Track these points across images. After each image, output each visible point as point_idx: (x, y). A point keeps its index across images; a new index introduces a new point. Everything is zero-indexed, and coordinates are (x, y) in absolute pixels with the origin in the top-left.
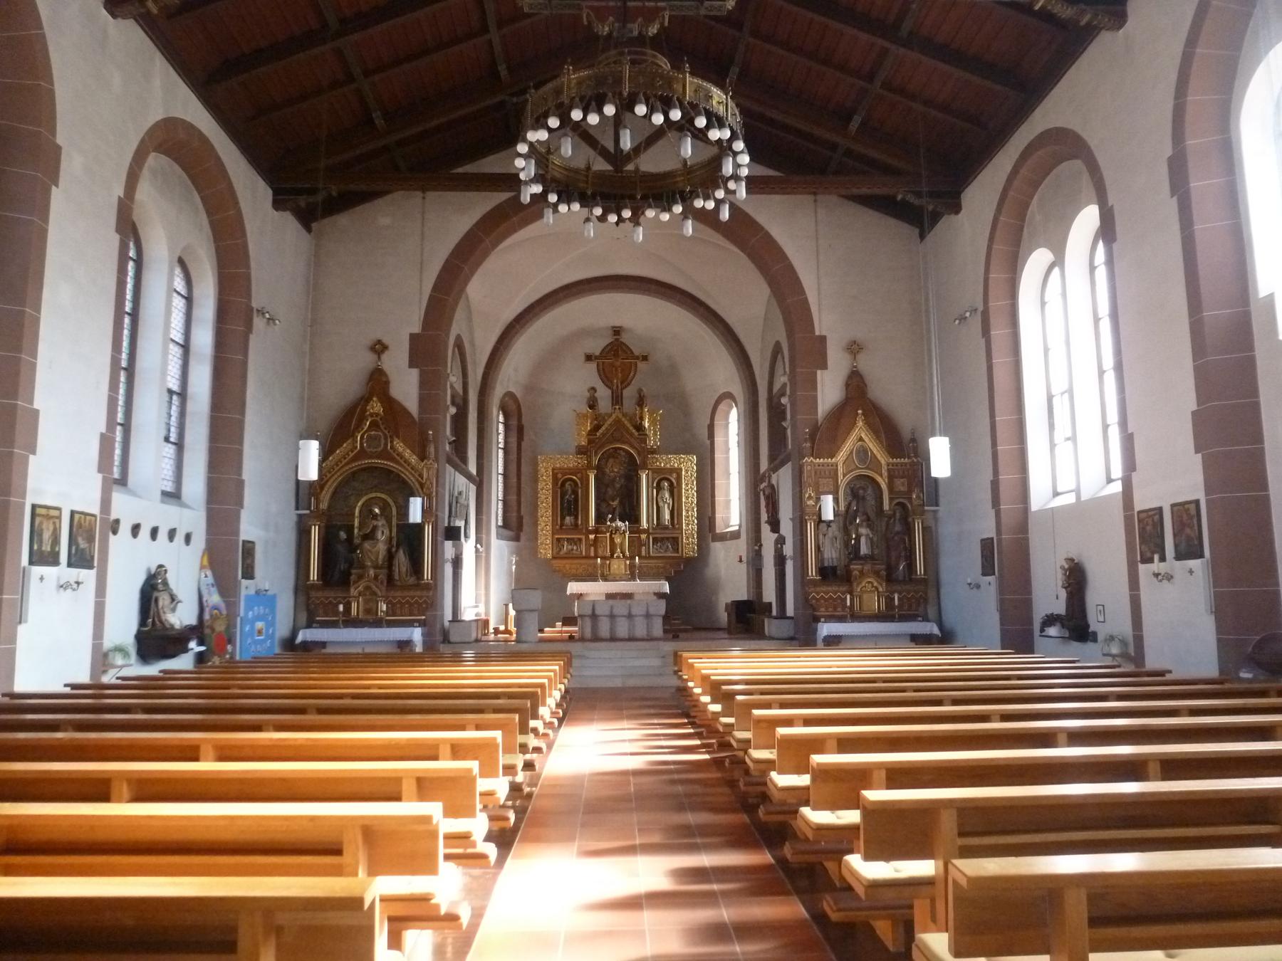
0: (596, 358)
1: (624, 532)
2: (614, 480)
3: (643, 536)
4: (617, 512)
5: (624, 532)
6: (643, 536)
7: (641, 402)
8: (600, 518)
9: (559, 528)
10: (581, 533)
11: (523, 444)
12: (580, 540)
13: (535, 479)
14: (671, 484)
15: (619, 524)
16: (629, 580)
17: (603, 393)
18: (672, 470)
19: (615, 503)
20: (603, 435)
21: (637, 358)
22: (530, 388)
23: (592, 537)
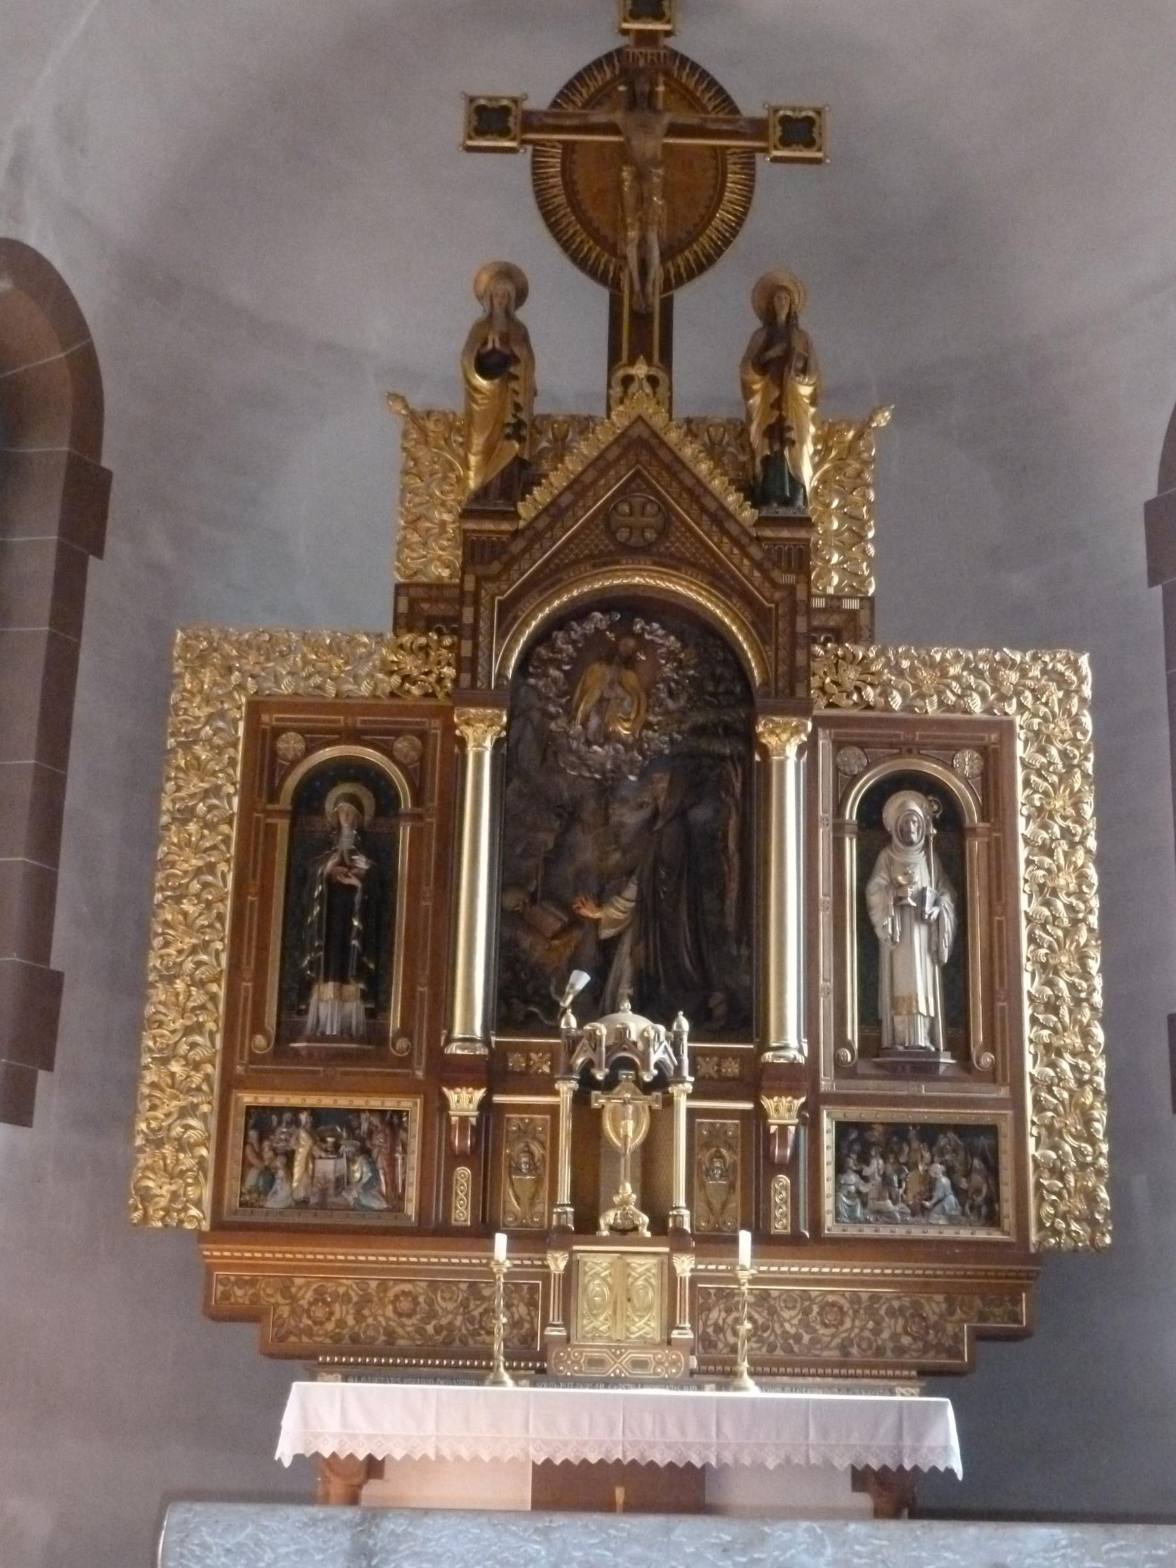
0: (530, 122)
1: (662, 1082)
2: (607, 788)
3: (782, 1110)
4: (623, 966)
5: (662, 1082)
6: (782, 1110)
7: (776, 351)
8: (522, 996)
9: (267, 1030)
10: (411, 1089)
11: (100, 577)
12: (394, 1122)
13: (144, 773)
14: (949, 824)
15: (637, 1025)
16: (694, 1379)
17: (568, 331)
18: (949, 735)
19: (615, 913)
20: (555, 512)
21: (758, 128)
22: (151, 280)
23: (464, 1101)
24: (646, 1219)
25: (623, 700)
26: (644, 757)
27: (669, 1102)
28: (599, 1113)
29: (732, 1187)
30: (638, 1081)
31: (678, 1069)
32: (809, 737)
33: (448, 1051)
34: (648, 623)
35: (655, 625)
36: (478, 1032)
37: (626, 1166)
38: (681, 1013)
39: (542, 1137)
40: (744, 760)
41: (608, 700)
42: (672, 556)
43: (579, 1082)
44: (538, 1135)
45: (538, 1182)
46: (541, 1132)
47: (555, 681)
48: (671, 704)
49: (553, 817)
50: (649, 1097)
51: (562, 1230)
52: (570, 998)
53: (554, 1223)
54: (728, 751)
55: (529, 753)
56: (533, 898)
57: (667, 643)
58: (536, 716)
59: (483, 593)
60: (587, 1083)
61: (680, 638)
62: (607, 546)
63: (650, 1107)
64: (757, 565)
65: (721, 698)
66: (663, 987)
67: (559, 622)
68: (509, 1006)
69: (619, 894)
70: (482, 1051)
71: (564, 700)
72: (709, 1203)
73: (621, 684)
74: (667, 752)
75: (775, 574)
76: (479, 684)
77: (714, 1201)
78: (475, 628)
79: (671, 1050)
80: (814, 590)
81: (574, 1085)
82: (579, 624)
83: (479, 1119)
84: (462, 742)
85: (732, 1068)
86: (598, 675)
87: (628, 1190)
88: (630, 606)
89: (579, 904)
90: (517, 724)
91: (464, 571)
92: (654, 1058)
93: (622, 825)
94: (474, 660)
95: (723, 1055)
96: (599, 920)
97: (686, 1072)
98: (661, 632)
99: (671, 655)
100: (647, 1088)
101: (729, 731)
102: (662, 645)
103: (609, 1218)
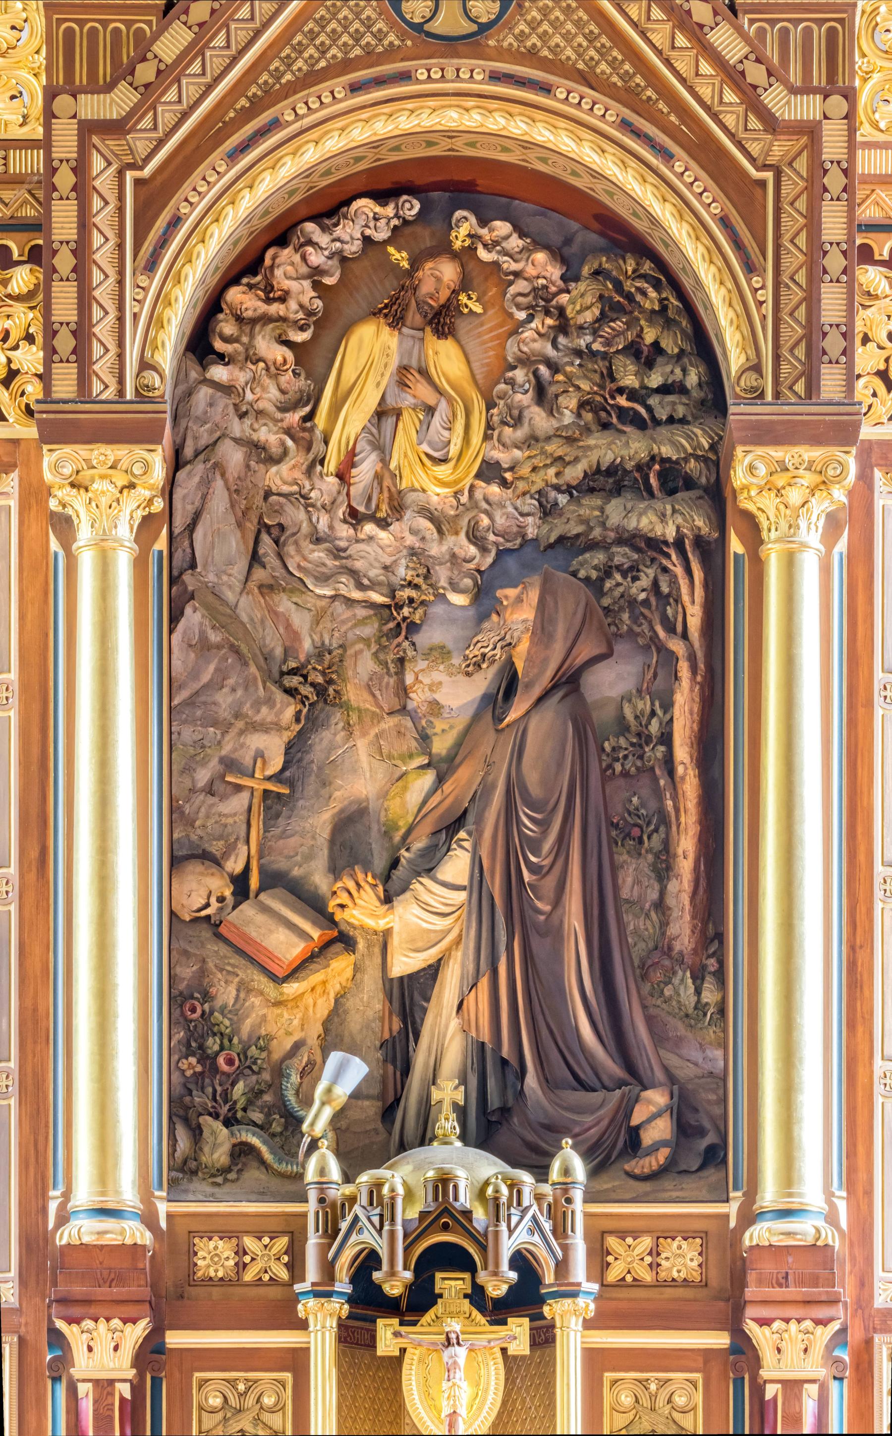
5: (527, 1294)
25: (430, 410)
26: (484, 550)
27: (544, 1337)
30: (477, 1296)
31: (562, 1267)
32: (850, 494)
33: (64, 1237)
34: (483, 222)
35: (502, 227)
36: (128, 1193)
38: (567, 1142)
40: (711, 552)
41: (398, 414)
42: (531, 56)
43: (351, 1300)
47: (275, 371)
48: (539, 419)
49: (279, 696)
52: (327, 1113)
54: (670, 533)
55: (221, 547)
56: (240, 883)
57: (531, 271)
58: (234, 457)
59: (97, 163)
61: (558, 254)
62: (379, 36)
64: (733, 76)
65: (653, 401)
66: (531, 1080)
67: (280, 231)
68: (196, 1133)
69: (430, 871)
70: (135, 1232)
71: (294, 418)
73: (424, 373)
74: (531, 532)
75: (775, 99)
76: (97, 387)
78: (82, 250)
79: (547, 1226)
80: (865, 132)
82: (324, 229)
83: (137, 1388)
84: (63, 525)
85: (683, 1260)
86: (371, 350)
88: (441, 186)
89: (343, 898)
90: (190, 480)
91: (49, 115)
93: (435, 707)
94: (82, 332)
95: (663, 1232)
96: (387, 934)
98: (515, 243)
99: (542, 300)
100: (497, 1311)
101: (672, 480)
102: (517, 274)
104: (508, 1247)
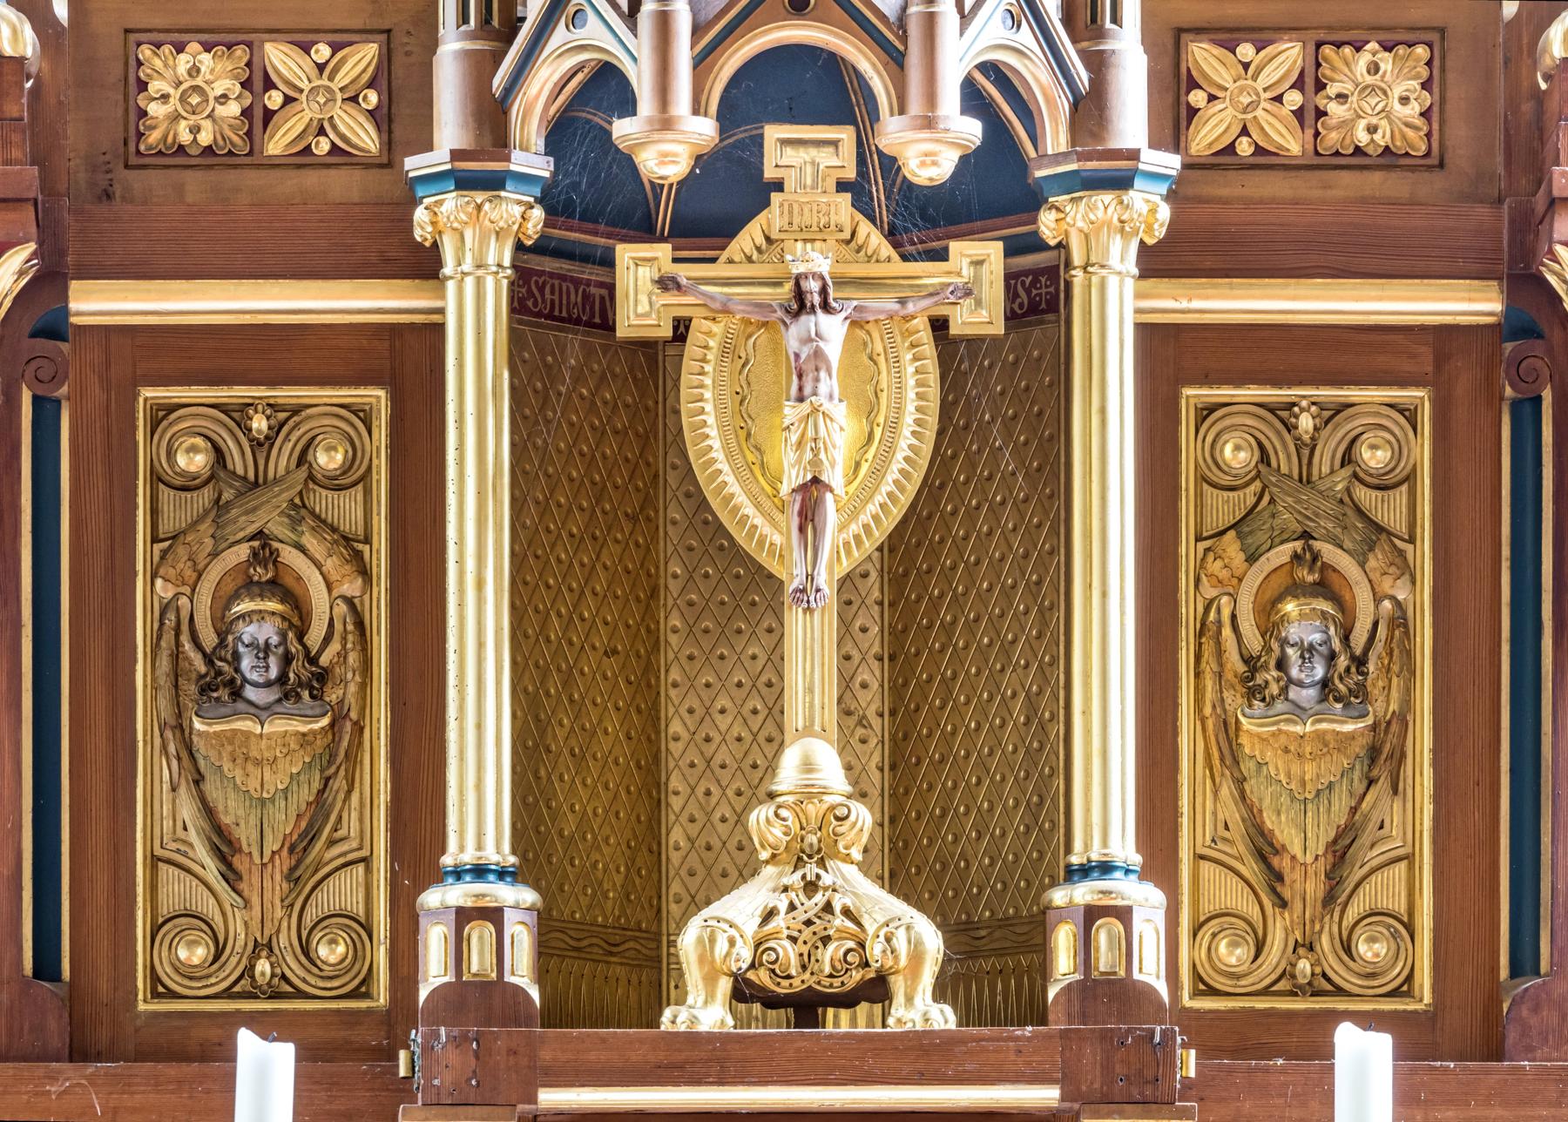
24: (933, 941)
27: (1041, 295)
28: (656, 360)
29: (1381, 757)
31: (1090, 109)
37: (810, 651)
39: (345, 509)
43: (552, 199)
44: (322, 500)
45: (335, 755)
46: (335, 483)
50: (929, 273)
51: (478, 1000)
53: (435, 972)
60: (595, 199)
63: (939, 325)
72: (1265, 848)
77: (1285, 832)
81: (518, 213)
87: (815, 763)
92: (957, 56)
97: (1131, 121)
103: (724, 933)
104: (957, 56)
